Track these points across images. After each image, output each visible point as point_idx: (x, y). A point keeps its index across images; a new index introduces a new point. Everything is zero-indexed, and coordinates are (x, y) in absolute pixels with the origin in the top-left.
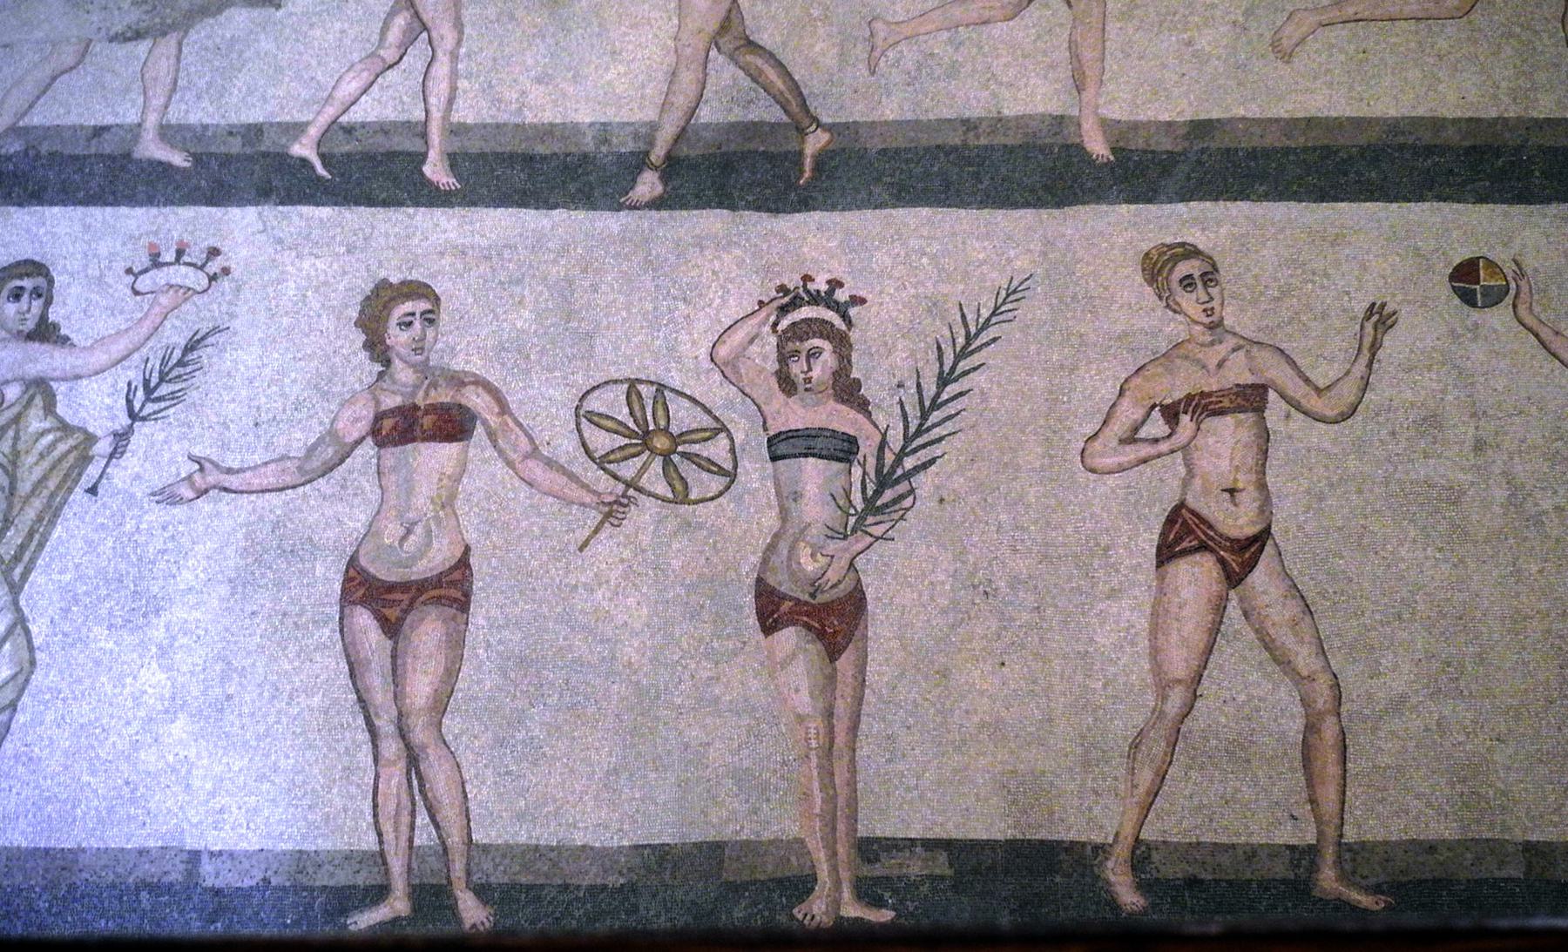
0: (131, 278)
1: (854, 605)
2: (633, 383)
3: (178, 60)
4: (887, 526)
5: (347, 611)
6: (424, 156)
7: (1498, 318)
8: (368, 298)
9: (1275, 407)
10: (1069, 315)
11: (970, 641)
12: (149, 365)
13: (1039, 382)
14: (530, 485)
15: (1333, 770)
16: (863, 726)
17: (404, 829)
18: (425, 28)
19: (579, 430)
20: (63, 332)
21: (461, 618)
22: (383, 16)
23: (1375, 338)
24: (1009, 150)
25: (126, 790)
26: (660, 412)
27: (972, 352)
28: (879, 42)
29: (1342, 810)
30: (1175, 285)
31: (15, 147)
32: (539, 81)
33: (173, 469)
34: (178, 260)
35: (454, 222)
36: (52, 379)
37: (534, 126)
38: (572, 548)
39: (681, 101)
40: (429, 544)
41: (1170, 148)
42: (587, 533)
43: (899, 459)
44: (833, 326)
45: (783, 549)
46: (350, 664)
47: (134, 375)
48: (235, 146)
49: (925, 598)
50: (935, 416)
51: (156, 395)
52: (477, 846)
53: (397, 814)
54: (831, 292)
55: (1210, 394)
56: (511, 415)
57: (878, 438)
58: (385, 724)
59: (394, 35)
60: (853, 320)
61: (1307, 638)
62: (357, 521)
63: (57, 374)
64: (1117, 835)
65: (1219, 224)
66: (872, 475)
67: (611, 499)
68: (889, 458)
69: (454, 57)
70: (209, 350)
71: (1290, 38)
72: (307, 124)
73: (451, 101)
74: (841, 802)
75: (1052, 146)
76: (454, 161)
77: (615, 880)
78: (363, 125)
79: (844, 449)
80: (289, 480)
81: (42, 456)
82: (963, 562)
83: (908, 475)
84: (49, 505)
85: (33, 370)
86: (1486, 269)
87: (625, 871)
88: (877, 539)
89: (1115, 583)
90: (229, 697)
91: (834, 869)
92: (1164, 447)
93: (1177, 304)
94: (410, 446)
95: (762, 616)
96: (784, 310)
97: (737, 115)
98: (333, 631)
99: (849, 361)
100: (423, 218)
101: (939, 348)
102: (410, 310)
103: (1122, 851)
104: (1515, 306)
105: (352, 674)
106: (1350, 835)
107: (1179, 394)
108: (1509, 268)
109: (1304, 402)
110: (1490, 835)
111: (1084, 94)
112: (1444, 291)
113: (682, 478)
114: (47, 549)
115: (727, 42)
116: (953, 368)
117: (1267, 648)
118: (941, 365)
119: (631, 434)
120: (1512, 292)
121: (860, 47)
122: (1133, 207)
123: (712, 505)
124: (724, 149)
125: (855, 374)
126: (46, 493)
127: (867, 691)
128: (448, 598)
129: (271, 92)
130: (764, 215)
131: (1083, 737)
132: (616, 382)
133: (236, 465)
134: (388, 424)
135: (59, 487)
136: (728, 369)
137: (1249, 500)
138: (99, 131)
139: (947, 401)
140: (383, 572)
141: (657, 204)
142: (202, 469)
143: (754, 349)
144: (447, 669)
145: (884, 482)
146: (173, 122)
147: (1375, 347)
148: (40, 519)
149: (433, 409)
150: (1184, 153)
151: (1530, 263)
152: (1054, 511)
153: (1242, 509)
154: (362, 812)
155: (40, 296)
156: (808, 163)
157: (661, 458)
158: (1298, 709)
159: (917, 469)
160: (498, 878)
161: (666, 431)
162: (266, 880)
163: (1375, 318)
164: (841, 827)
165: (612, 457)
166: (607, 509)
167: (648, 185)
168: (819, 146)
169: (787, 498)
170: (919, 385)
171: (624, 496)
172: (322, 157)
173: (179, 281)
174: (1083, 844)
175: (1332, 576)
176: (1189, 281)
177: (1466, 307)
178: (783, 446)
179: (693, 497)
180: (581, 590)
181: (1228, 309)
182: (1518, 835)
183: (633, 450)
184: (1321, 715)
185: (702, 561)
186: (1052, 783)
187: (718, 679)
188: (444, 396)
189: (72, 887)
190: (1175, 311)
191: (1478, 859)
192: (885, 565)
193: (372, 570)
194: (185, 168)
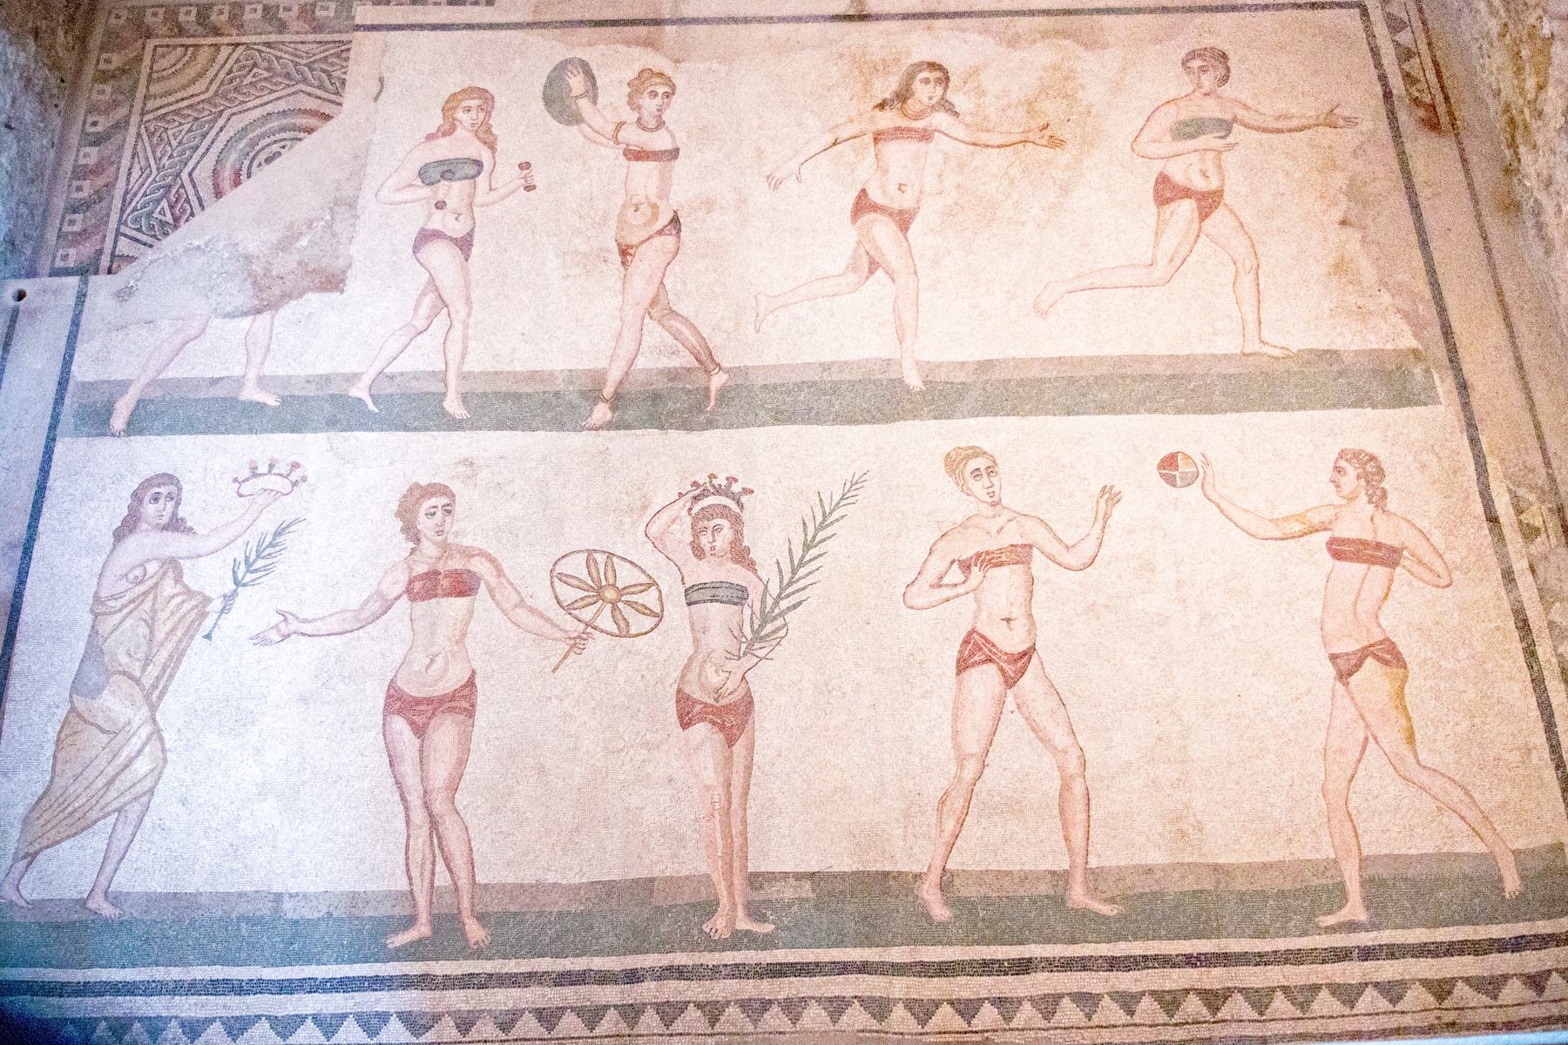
0: (237, 485)
1: (746, 705)
2: (590, 552)
6: (444, 394)
8: (405, 496)
9: (1038, 560)
12: (249, 547)
15: (1082, 817)
16: (751, 792)
17: (427, 874)
22: (416, 297)
24: (853, 384)
26: (610, 573)
30: (967, 475)
34: (270, 472)
38: (548, 670)
40: (445, 670)
43: (776, 603)
44: (730, 509)
45: (695, 667)
46: (389, 756)
48: (311, 391)
49: (795, 700)
51: (253, 568)
52: (480, 885)
53: (423, 864)
55: (993, 553)
56: (505, 576)
58: (415, 800)
59: (424, 311)
63: (185, 554)
66: (758, 615)
67: (575, 635)
68: (770, 601)
69: (466, 325)
73: (463, 356)
74: (737, 845)
76: (465, 399)
79: (739, 596)
81: (172, 613)
83: (782, 614)
84: (177, 648)
85: (167, 552)
90: (303, 783)
91: (731, 895)
92: (960, 590)
93: (969, 489)
95: (681, 717)
96: (696, 499)
99: (742, 534)
101: (804, 523)
102: (434, 504)
103: (934, 877)
104: (1203, 486)
105: (391, 764)
106: (1093, 862)
107: (970, 553)
108: (1198, 459)
111: (905, 345)
116: (814, 537)
118: (806, 535)
120: (1201, 477)
125: (746, 543)
126: (175, 639)
132: (578, 552)
133: (310, 617)
134: (417, 586)
135: (184, 635)
137: (1020, 626)
138: (215, 381)
139: (810, 561)
140: (412, 690)
141: (610, 426)
143: (675, 527)
146: (268, 374)
147: (1106, 517)
148: (171, 656)
156: (713, 394)
157: (610, 605)
158: (1057, 773)
160: (494, 908)
161: (614, 585)
162: (330, 914)
163: (1107, 496)
164: (736, 865)
165: (576, 605)
166: (572, 642)
167: (602, 412)
169: (698, 632)
170: (790, 550)
172: (372, 396)
174: (907, 874)
176: (977, 473)
178: (695, 595)
179: (633, 631)
183: (590, 600)
188: (456, 564)
189: (193, 921)
193: (406, 689)
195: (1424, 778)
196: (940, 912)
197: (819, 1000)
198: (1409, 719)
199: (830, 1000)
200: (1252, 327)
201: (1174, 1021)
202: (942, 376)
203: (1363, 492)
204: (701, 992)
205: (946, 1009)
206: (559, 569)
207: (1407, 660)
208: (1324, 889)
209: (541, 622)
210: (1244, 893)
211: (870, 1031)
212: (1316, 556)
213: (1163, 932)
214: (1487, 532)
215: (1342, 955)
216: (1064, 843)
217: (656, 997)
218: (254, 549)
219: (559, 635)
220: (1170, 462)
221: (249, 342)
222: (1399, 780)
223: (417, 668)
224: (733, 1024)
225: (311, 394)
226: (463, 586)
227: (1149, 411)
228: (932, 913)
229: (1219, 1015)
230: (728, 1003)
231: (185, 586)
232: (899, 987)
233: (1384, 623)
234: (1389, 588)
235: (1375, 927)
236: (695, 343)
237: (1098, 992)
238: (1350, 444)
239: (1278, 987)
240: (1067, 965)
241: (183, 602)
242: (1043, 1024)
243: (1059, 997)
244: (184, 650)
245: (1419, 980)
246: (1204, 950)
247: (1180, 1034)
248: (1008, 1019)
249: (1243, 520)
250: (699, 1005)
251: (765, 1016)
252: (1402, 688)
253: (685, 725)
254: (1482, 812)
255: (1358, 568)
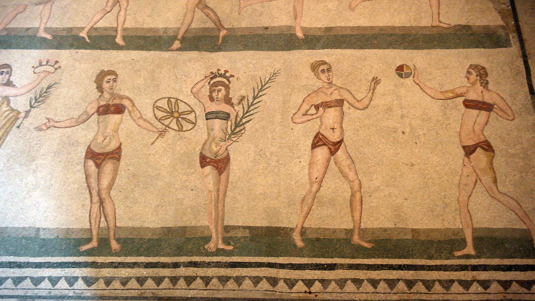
0: (33, 69)
1: (227, 159)
2: (169, 98)
3: (51, 10)
4: (237, 138)
5: (86, 161)
6: (116, 36)
7: (409, 81)
8: (98, 75)
10: (290, 80)
11: (258, 170)
12: (37, 93)
13: (281, 98)
14: (139, 126)
15: (359, 207)
16: (227, 194)
17: (98, 222)
18: (119, 2)
19: (154, 111)
20: (14, 83)
21: (118, 163)
23: (374, 87)
25: (21, 210)
26: (176, 106)
27: (263, 90)
28: (242, 6)
29: (361, 219)
30: (319, 72)
31: (4, 33)
32: (148, 16)
33: (41, 121)
35: (123, 54)
36: (11, 96)
37: (146, 29)
38: (150, 143)
39: (187, 22)
40: (110, 142)
41: (320, 35)
42: (154, 139)
43: (241, 120)
45: (208, 144)
46: (86, 175)
47: (33, 96)
48: (65, 33)
50: (252, 108)
52: (118, 227)
53: (96, 218)
54: (225, 74)
55: (328, 102)
56: (135, 107)
57: (236, 114)
58: (94, 193)
60: (231, 81)
61: (352, 170)
62: (91, 135)
63: (11, 95)
64: (297, 226)
65: (332, 55)
68: (239, 119)
69: (126, 10)
70: (53, 89)
71: (354, 5)
72: (85, 28)
73: (124, 21)
74: (220, 215)
75: (288, 34)
76: (124, 38)
77: (156, 237)
78: (100, 28)
79: (226, 117)
80: (73, 124)
81: (5, 118)
82: (257, 148)
83: (243, 124)
84: (6, 131)
85: (5, 94)
86: (406, 67)
87: (158, 234)
88: (234, 141)
89: (299, 154)
90: (52, 185)
91: (217, 234)
92: (314, 116)
94: (107, 115)
95: (201, 163)
96: (212, 79)
97: (202, 26)
98: (82, 166)
99: (229, 93)
100: (114, 53)
101: (254, 89)
102: (109, 78)
103: (298, 230)
105: (86, 178)
106: (363, 226)
107: (319, 102)
108: (412, 67)
109: (354, 104)
110: (402, 227)
112: (394, 74)
113: (181, 125)
114: (4, 143)
115: (200, 6)
116: (257, 95)
117: (341, 173)
118: (254, 94)
119: (168, 112)
120: (413, 74)
121: (236, 7)
122: (309, 51)
123: (190, 131)
124: (198, 35)
125: (230, 96)
126: (5, 128)
127: (229, 184)
128: (114, 157)
129: (76, 19)
130: (208, 53)
131: (289, 198)
132: (165, 98)
134: (101, 109)
135: (9, 126)
136: (195, 95)
137: (338, 132)
138: (28, 29)
139: (255, 104)
140: (97, 150)
142: (49, 121)
143: (203, 89)
144: (113, 177)
145: (237, 125)
146: (48, 27)
147: (374, 89)
149: (114, 105)
150: (323, 36)
151: (418, 66)
152: (284, 134)
153: (336, 134)
154: (86, 217)
155: (8, 74)
156: (221, 38)
158: (350, 190)
159: (246, 122)
160: (123, 236)
161: (178, 111)
162: (58, 236)
163: (375, 81)
164: (220, 222)
165: (162, 119)
166: (160, 133)
167: (177, 44)
168: (224, 34)
169: (210, 130)
171: (165, 129)
172: (88, 36)
173: (46, 70)
174: (287, 228)
175: (360, 153)
177: (400, 78)
178: (210, 116)
179: (184, 129)
180: (151, 155)
181: (334, 79)
182: (411, 227)
183: (168, 117)
184: (356, 192)
185: (185, 148)
186: (279, 211)
187: (188, 180)
188: (117, 102)
190: (319, 79)
191: (399, 233)
192: (236, 149)
193: (94, 149)
194: (50, 39)
195: (498, 196)
196: (300, 243)
197: (250, 278)
198: (494, 172)
199: (254, 277)
200: (436, 17)
201: (393, 292)
202: (311, 33)
203: (479, 82)
204: (203, 273)
205: (300, 283)
206: (156, 105)
207: (495, 149)
208: (458, 241)
209: (149, 125)
210: (423, 241)
211: (269, 291)
212: (458, 107)
213: (390, 255)
214: (530, 99)
215: (463, 268)
216: (351, 218)
217: (184, 274)
218: (39, 93)
219: (155, 130)
220: (400, 68)
221: (42, 14)
222: (490, 198)
223: (99, 141)
224: (214, 286)
225: (64, 35)
226: (119, 110)
227: (393, 48)
228: (297, 244)
229: (412, 290)
230: (213, 278)
231: (11, 107)
232: (282, 273)
233: (485, 134)
234: (488, 120)
235: (478, 256)
236: (215, 18)
237: (362, 278)
238: (475, 62)
239: (437, 280)
240: (351, 267)
241: (10, 113)
242: (340, 291)
243: (346, 280)
244: (9, 132)
245: (497, 280)
246: (406, 263)
247: (395, 297)
248: (325, 288)
249: (427, 91)
250: (202, 278)
251: (228, 283)
252: (492, 160)
253: (202, 167)
254: (525, 212)
255: (475, 112)
